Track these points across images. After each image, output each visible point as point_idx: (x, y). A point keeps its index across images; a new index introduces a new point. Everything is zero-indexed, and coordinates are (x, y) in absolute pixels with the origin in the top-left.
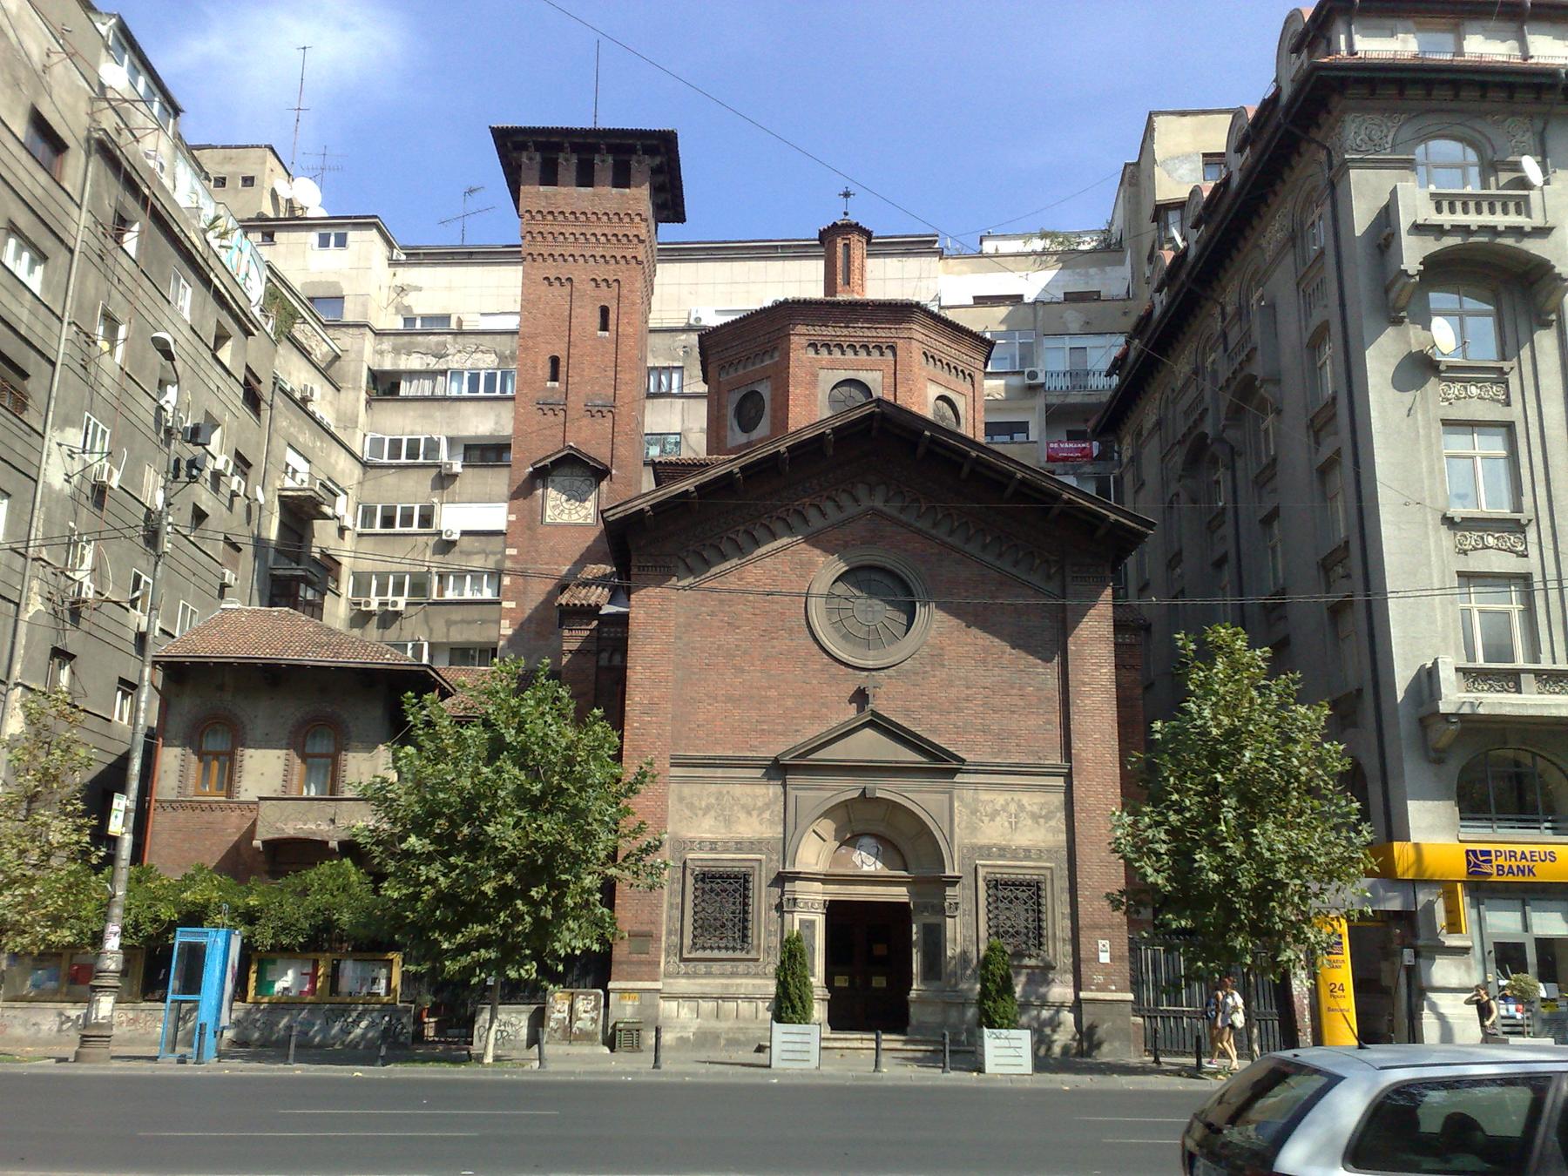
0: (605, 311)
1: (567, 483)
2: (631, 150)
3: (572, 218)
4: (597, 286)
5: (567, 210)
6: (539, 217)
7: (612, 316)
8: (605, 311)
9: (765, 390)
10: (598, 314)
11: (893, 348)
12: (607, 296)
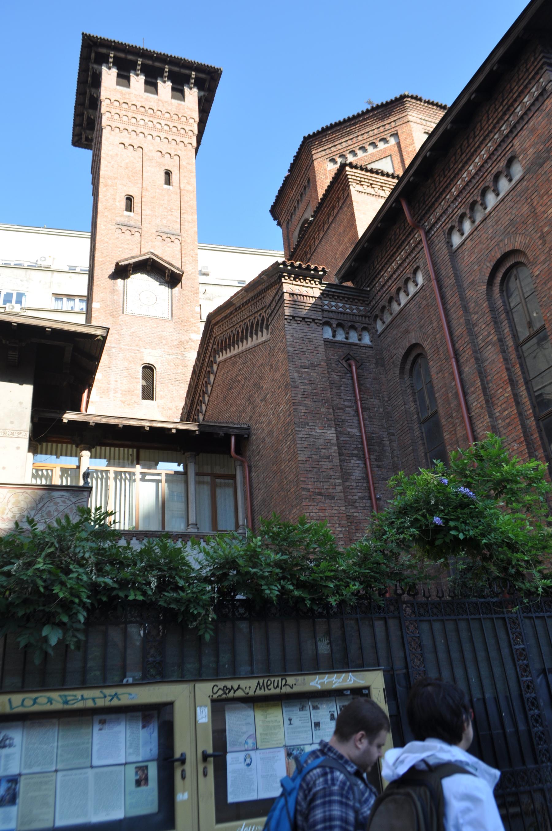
0: (168, 174)
5: (139, 105)
6: (116, 104)
7: (175, 178)
8: (168, 174)
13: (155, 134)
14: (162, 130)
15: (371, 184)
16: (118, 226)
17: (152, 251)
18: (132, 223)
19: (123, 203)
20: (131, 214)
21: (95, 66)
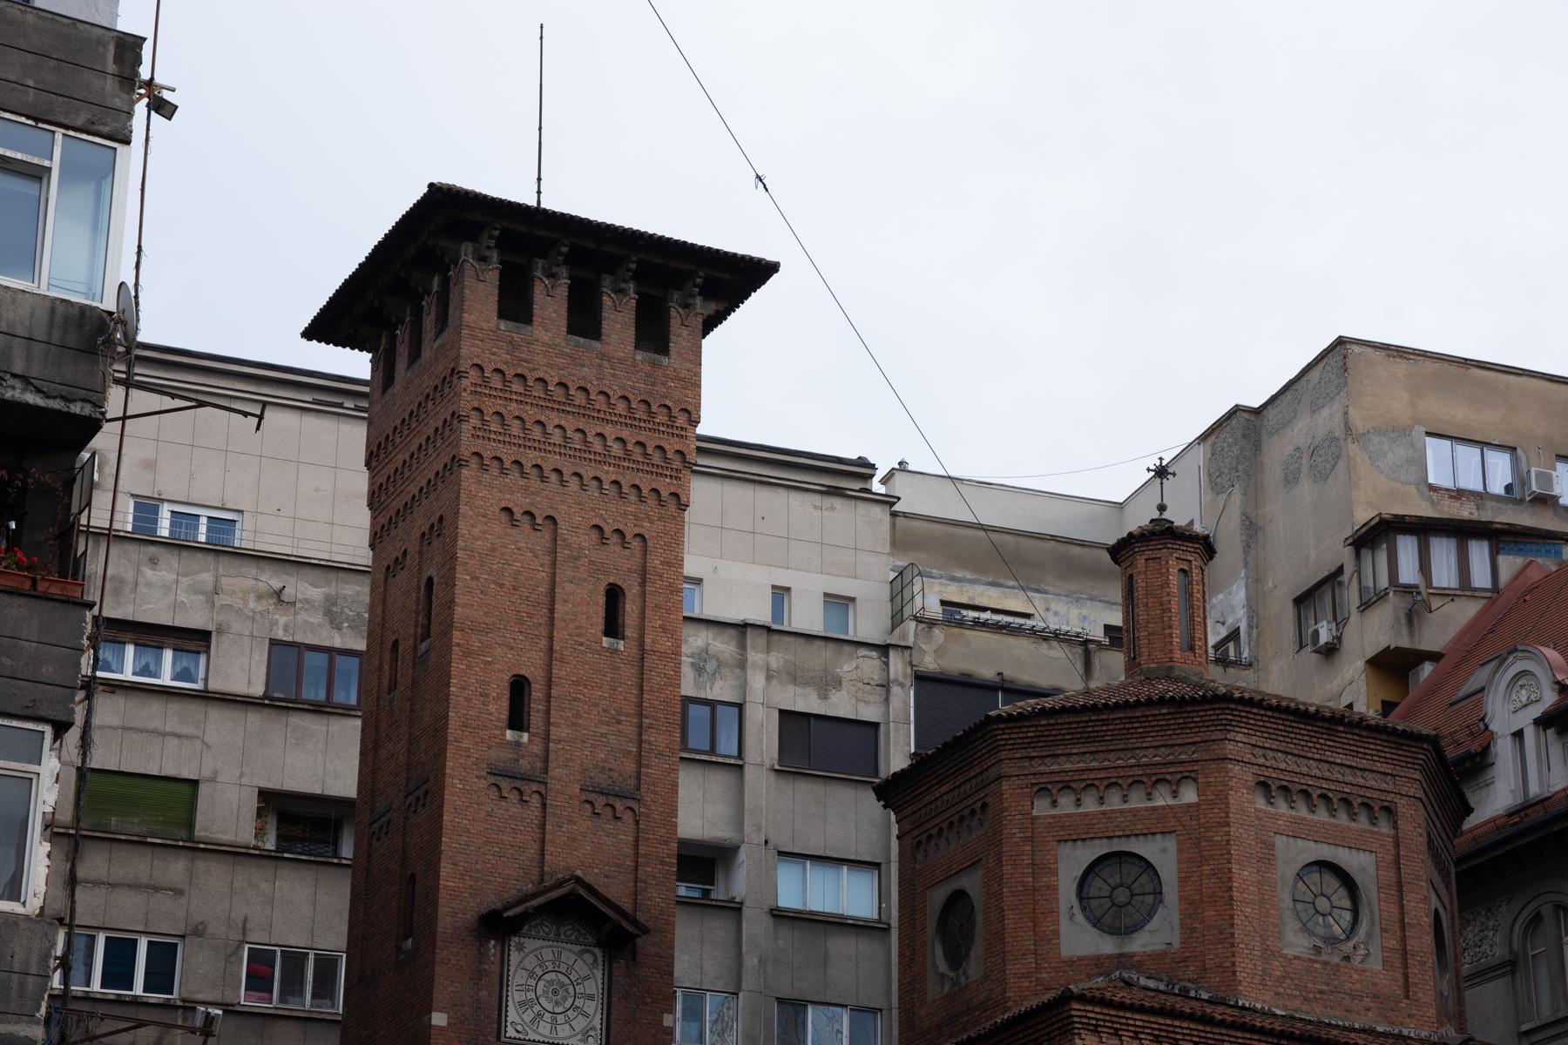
1: (547, 954)
2: (678, 280)
3: (559, 394)
4: (603, 539)
5: (553, 379)
6: (496, 381)
7: (630, 608)
8: (614, 595)
9: (1162, 853)
10: (602, 600)
11: (1389, 811)
12: (619, 564)
13: (588, 472)
14: (604, 458)
15: (1117, 1030)
16: (493, 779)
17: (579, 873)
18: (525, 765)
19: (500, 709)
20: (525, 737)
21: (443, 243)
